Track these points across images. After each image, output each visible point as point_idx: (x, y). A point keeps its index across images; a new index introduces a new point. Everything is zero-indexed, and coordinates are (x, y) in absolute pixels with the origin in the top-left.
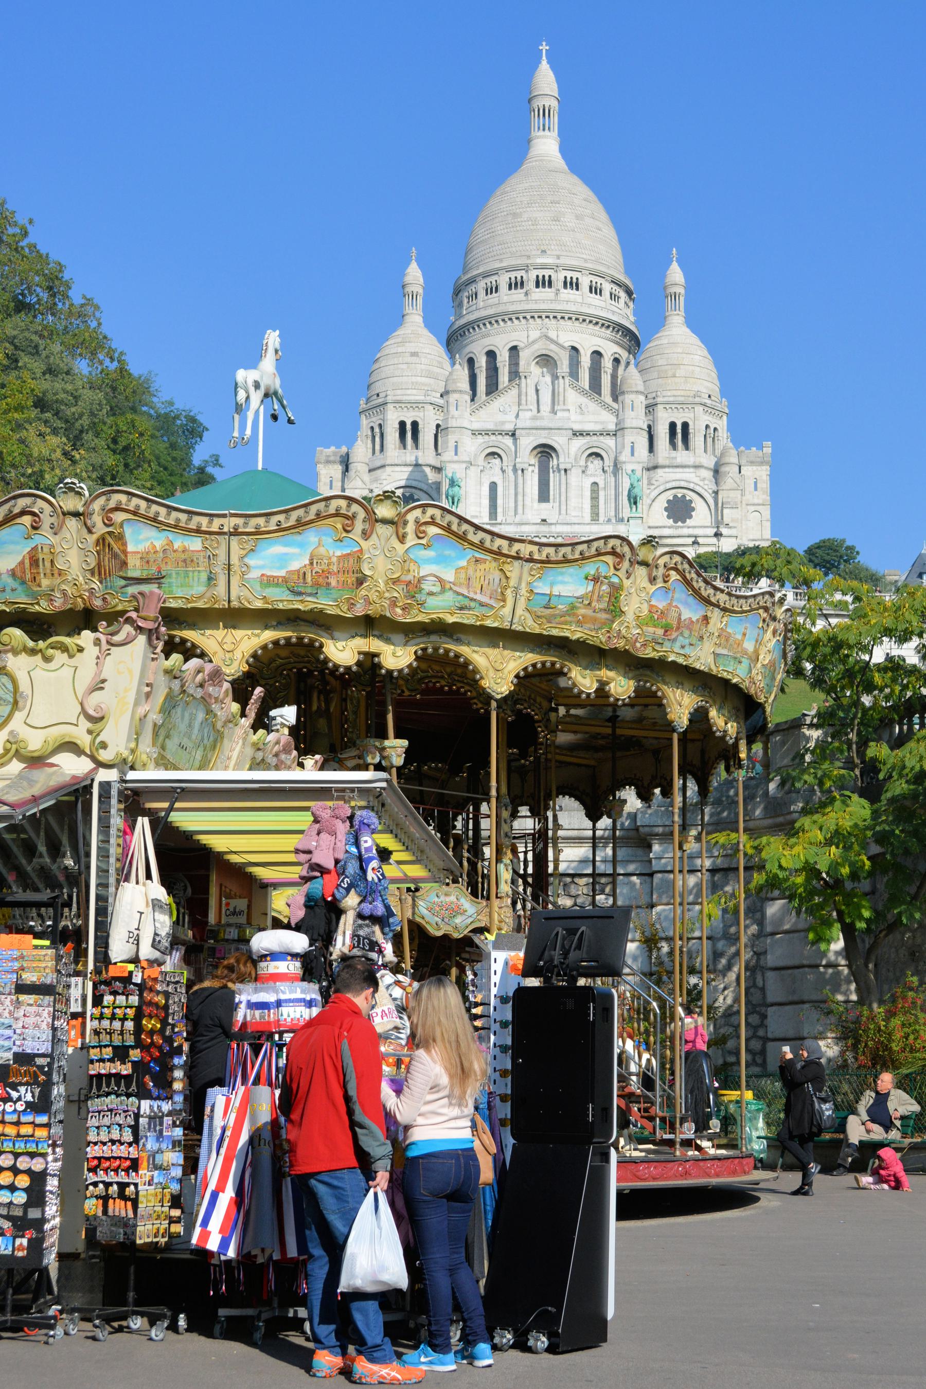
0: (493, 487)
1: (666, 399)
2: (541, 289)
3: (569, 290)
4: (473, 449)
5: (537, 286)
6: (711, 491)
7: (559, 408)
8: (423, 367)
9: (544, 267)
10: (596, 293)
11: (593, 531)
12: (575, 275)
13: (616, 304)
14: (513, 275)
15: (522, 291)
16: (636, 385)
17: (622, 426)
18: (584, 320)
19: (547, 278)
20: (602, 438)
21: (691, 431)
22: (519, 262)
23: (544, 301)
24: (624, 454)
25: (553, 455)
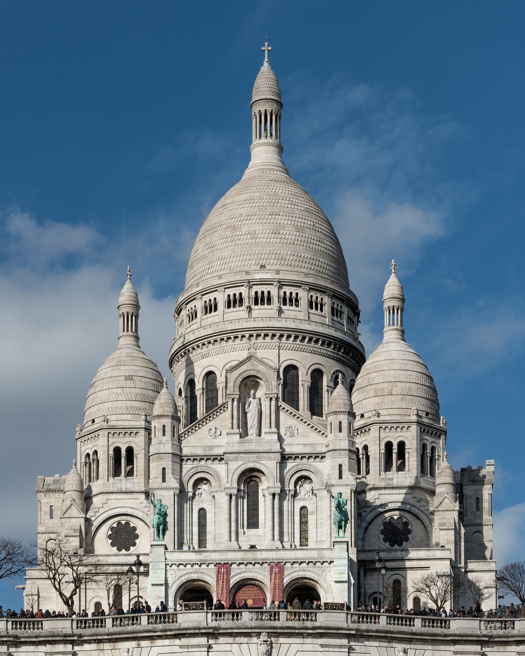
8: (138, 391)
11: (298, 556)
17: (331, 447)
18: (304, 338)
24: (332, 477)
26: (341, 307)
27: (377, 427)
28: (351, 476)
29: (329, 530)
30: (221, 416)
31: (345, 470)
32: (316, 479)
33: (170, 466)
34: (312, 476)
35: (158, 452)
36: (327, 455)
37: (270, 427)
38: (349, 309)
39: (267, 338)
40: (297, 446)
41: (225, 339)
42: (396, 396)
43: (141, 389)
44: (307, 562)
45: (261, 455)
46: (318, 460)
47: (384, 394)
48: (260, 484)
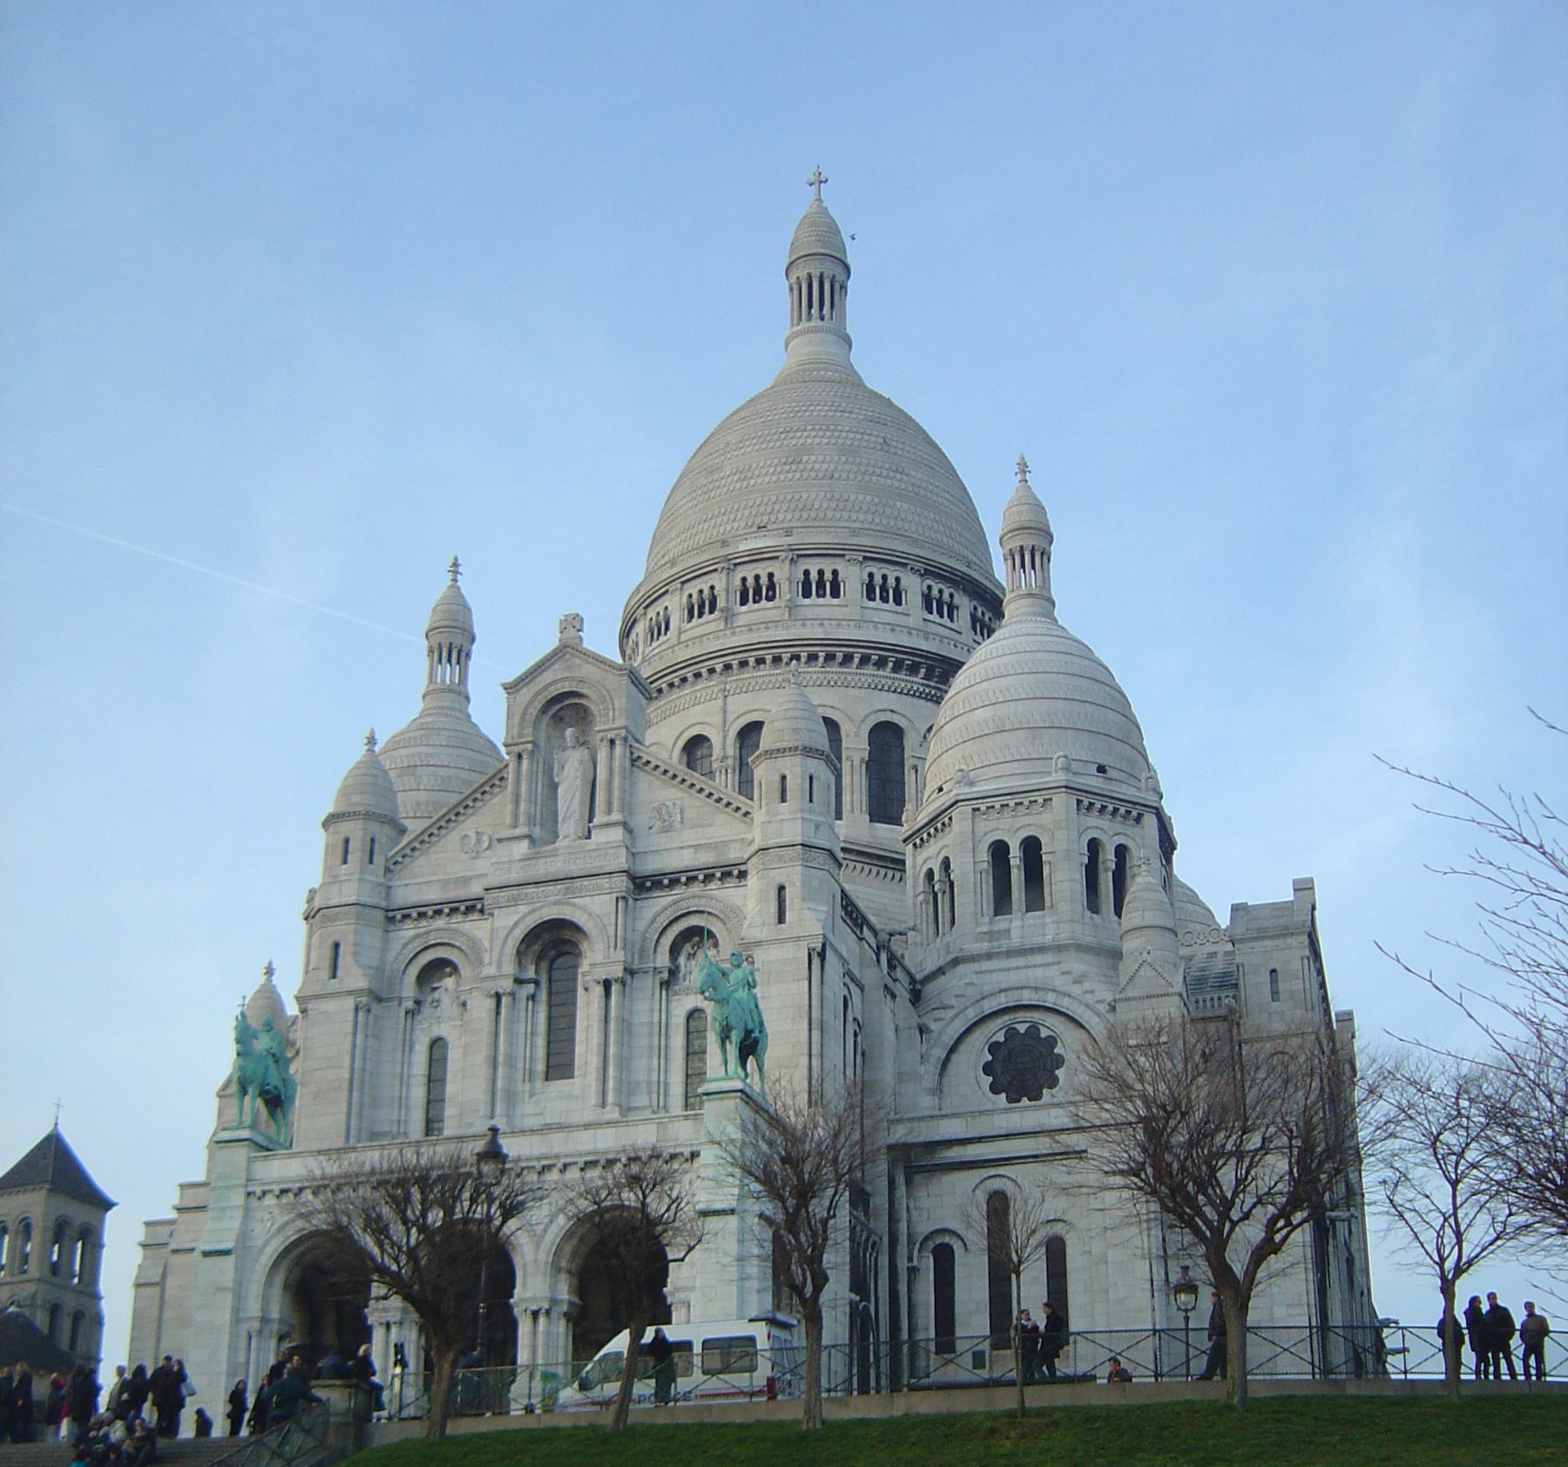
2: (751, 605)
5: (744, 602)
6: (1102, 1008)
8: (423, 796)
9: (756, 557)
10: (885, 600)
11: (601, 1146)
12: (828, 566)
13: (946, 620)
14: (692, 588)
18: (848, 659)
19: (764, 581)
21: (1044, 858)
22: (706, 557)
23: (750, 628)
25: (584, 946)
26: (951, 596)
27: (967, 809)
28: (808, 912)
30: (497, 800)
31: (792, 899)
32: (725, 933)
33: (351, 937)
34: (716, 927)
36: (751, 867)
37: (609, 812)
38: (975, 603)
39: (762, 666)
41: (677, 682)
43: (432, 793)
45: (576, 885)
46: (731, 882)
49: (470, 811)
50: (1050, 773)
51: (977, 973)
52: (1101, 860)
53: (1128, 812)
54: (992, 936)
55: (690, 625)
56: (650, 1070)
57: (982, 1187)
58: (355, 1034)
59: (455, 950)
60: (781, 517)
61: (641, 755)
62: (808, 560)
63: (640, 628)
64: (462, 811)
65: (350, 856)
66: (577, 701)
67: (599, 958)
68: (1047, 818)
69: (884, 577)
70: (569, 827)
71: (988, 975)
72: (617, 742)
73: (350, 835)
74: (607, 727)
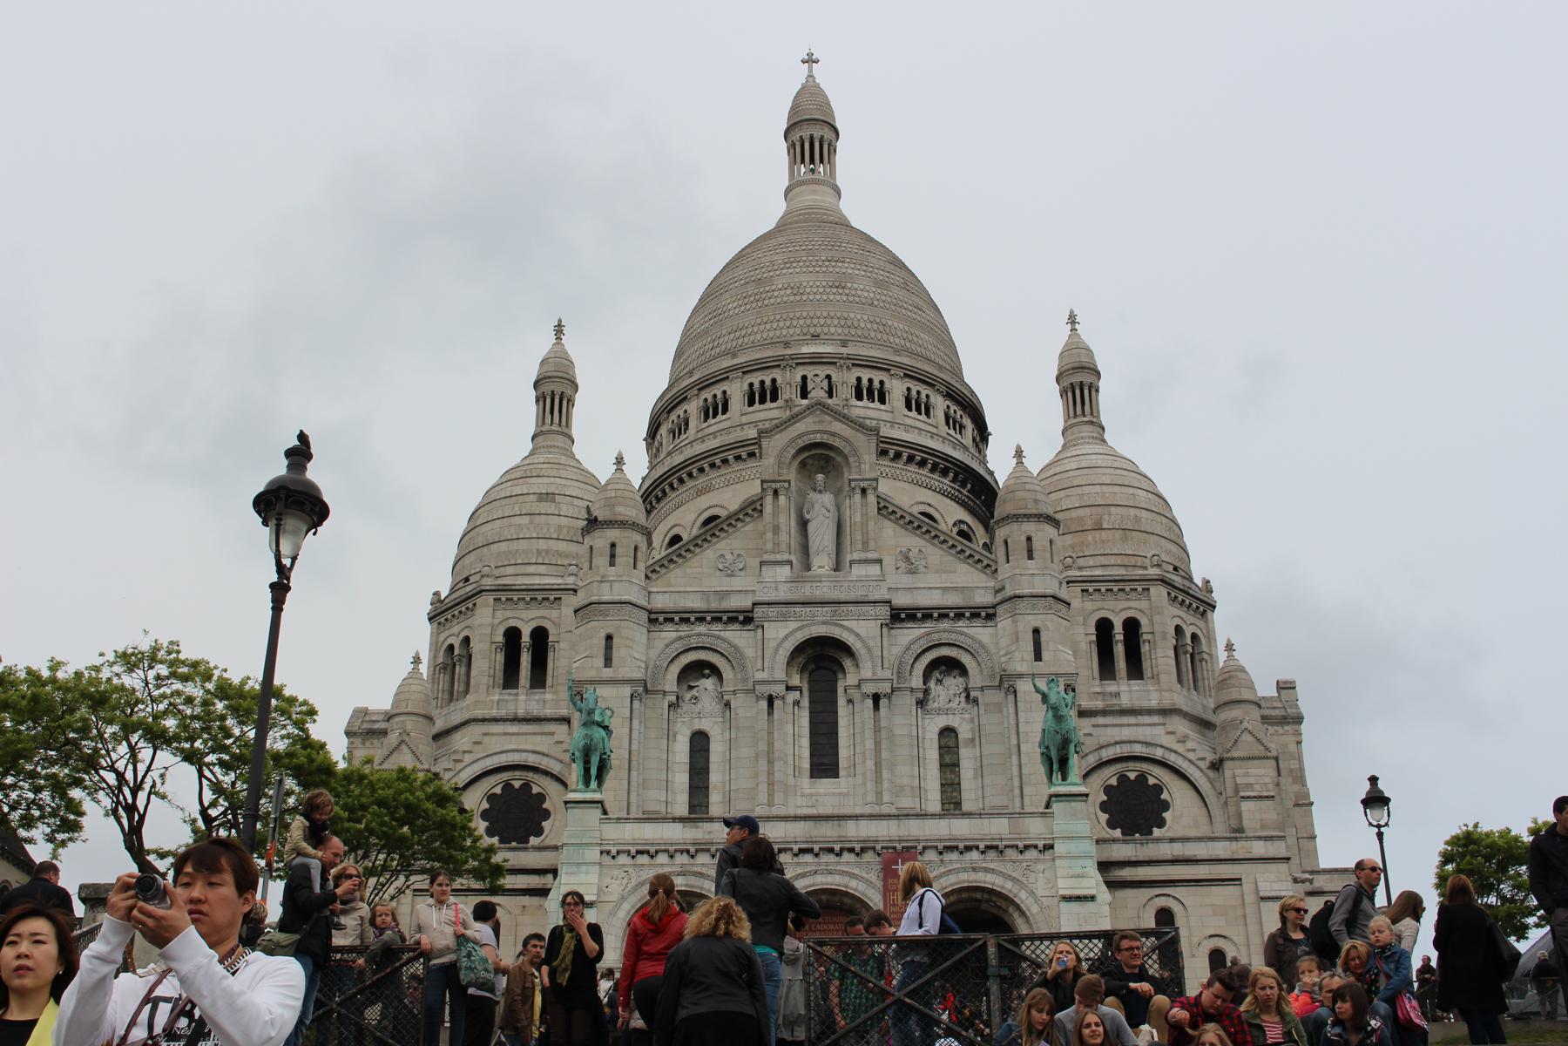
0: (700, 742)
1: (1084, 573)
3: (865, 402)
4: (653, 654)
6: (1202, 764)
7: (856, 556)
8: (564, 521)
9: (816, 360)
13: (958, 437)
14: (755, 379)
15: (774, 405)
16: (1035, 500)
17: (1009, 592)
18: (898, 456)
20: (961, 624)
21: (1145, 637)
22: (769, 353)
25: (847, 663)
26: (961, 416)
29: (1016, 783)
30: (746, 528)
32: (974, 664)
34: (965, 659)
35: (594, 599)
36: (1000, 610)
37: (865, 548)
40: (925, 591)
42: (1109, 532)
44: (982, 846)
46: (977, 622)
47: (1085, 528)
48: (840, 676)
49: (723, 535)
50: (1146, 568)
51: (1094, 726)
52: (1180, 643)
53: (1198, 608)
54: (1103, 694)
55: (751, 409)
56: (912, 776)
57: (1151, 902)
58: (631, 720)
59: (715, 655)
60: (833, 330)
61: (887, 505)
62: (859, 369)
63: (693, 407)
64: (718, 533)
65: (618, 560)
66: (824, 452)
67: (866, 673)
68: (1144, 604)
69: (918, 392)
70: (822, 562)
71: (1102, 729)
72: (868, 492)
73: (617, 541)
74: (858, 477)
